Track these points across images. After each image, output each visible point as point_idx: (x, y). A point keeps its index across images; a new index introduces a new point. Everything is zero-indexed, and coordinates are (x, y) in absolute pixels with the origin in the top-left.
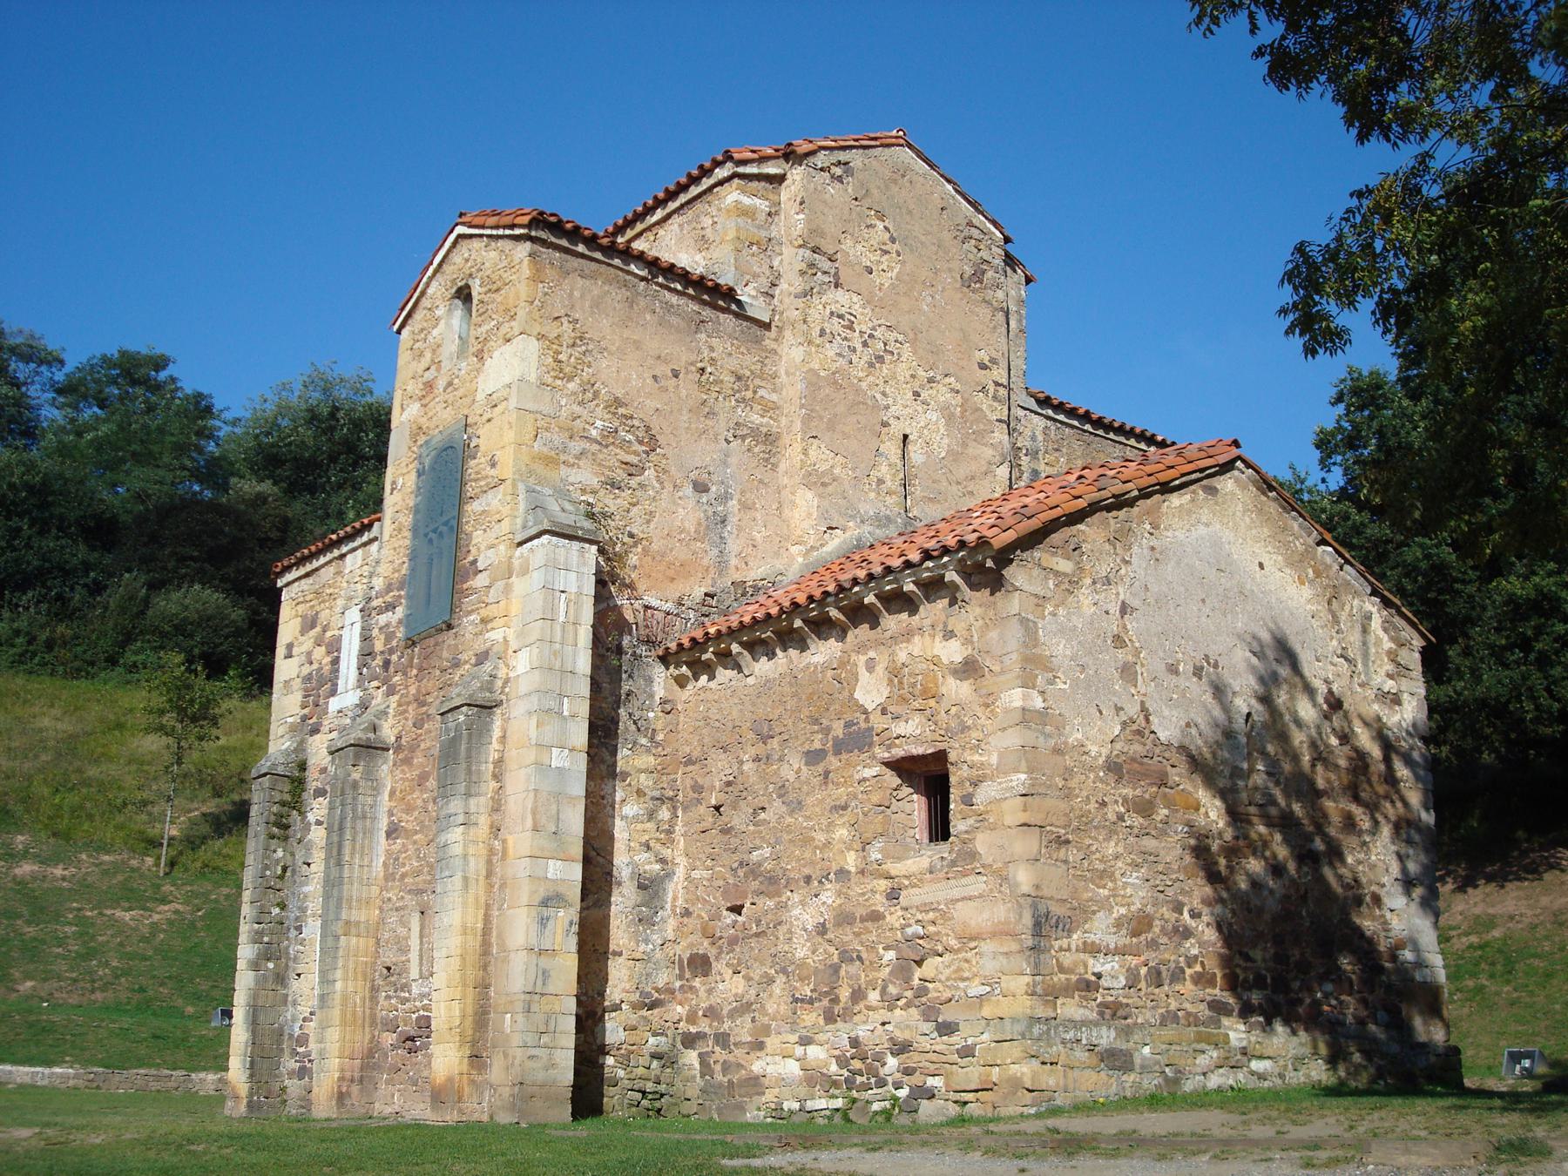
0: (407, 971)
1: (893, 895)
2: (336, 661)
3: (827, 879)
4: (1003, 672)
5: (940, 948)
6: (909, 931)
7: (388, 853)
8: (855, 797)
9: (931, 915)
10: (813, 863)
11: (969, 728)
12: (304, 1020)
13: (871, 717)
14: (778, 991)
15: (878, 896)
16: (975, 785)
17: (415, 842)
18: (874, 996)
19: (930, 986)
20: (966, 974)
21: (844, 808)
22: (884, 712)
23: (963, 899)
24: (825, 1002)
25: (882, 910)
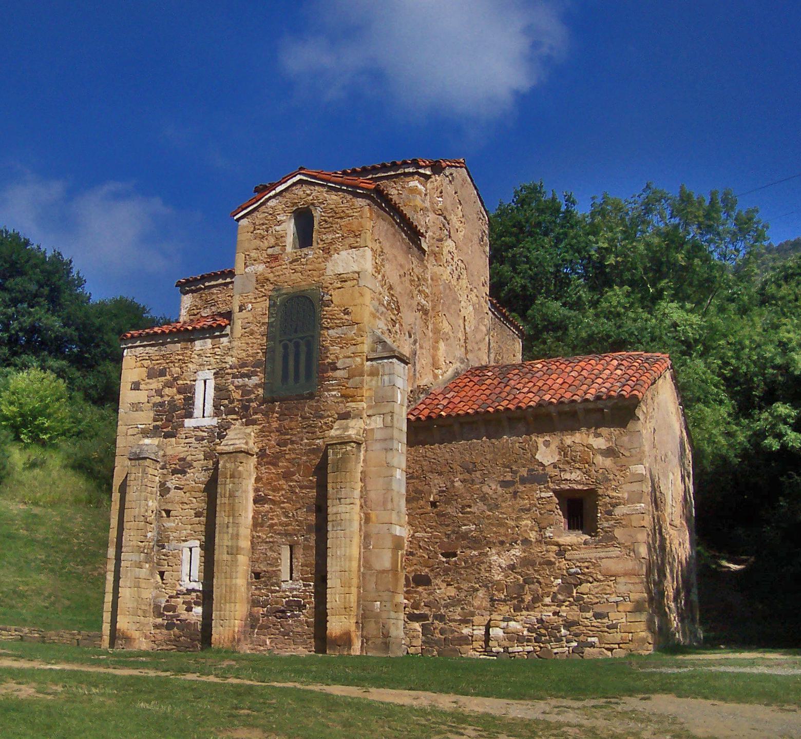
0: (277, 576)
1: (561, 553)
3: (516, 543)
4: (631, 456)
5: (591, 579)
6: (572, 571)
7: (256, 512)
8: (535, 506)
9: (586, 564)
10: (506, 535)
11: (610, 480)
12: (171, 597)
13: (547, 469)
14: (481, 595)
15: (551, 553)
16: (615, 505)
17: (283, 508)
18: (548, 600)
19: (585, 596)
20: (608, 592)
21: (529, 510)
22: (555, 467)
23: (607, 558)
24: (516, 602)
25: (553, 560)
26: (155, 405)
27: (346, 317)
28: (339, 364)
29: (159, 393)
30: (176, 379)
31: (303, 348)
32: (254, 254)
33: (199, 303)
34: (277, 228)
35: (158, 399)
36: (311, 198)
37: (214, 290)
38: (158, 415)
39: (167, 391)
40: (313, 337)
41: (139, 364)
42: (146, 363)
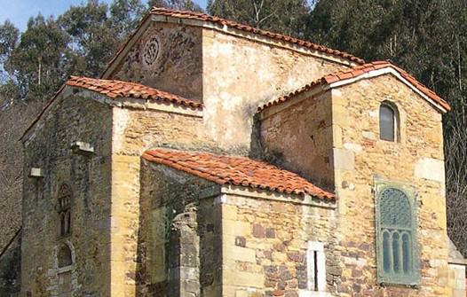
26: (265, 267)
27: (434, 220)
28: (432, 263)
29: (269, 255)
30: (286, 244)
31: (400, 241)
32: (350, 131)
33: (139, 126)
34: (372, 114)
35: (268, 263)
36: (398, 95)
37: (156, 115)
38: (270, 280)
39: (276, 255)
40: (409, 232)
41: (242, 217)
42: (251, 218)
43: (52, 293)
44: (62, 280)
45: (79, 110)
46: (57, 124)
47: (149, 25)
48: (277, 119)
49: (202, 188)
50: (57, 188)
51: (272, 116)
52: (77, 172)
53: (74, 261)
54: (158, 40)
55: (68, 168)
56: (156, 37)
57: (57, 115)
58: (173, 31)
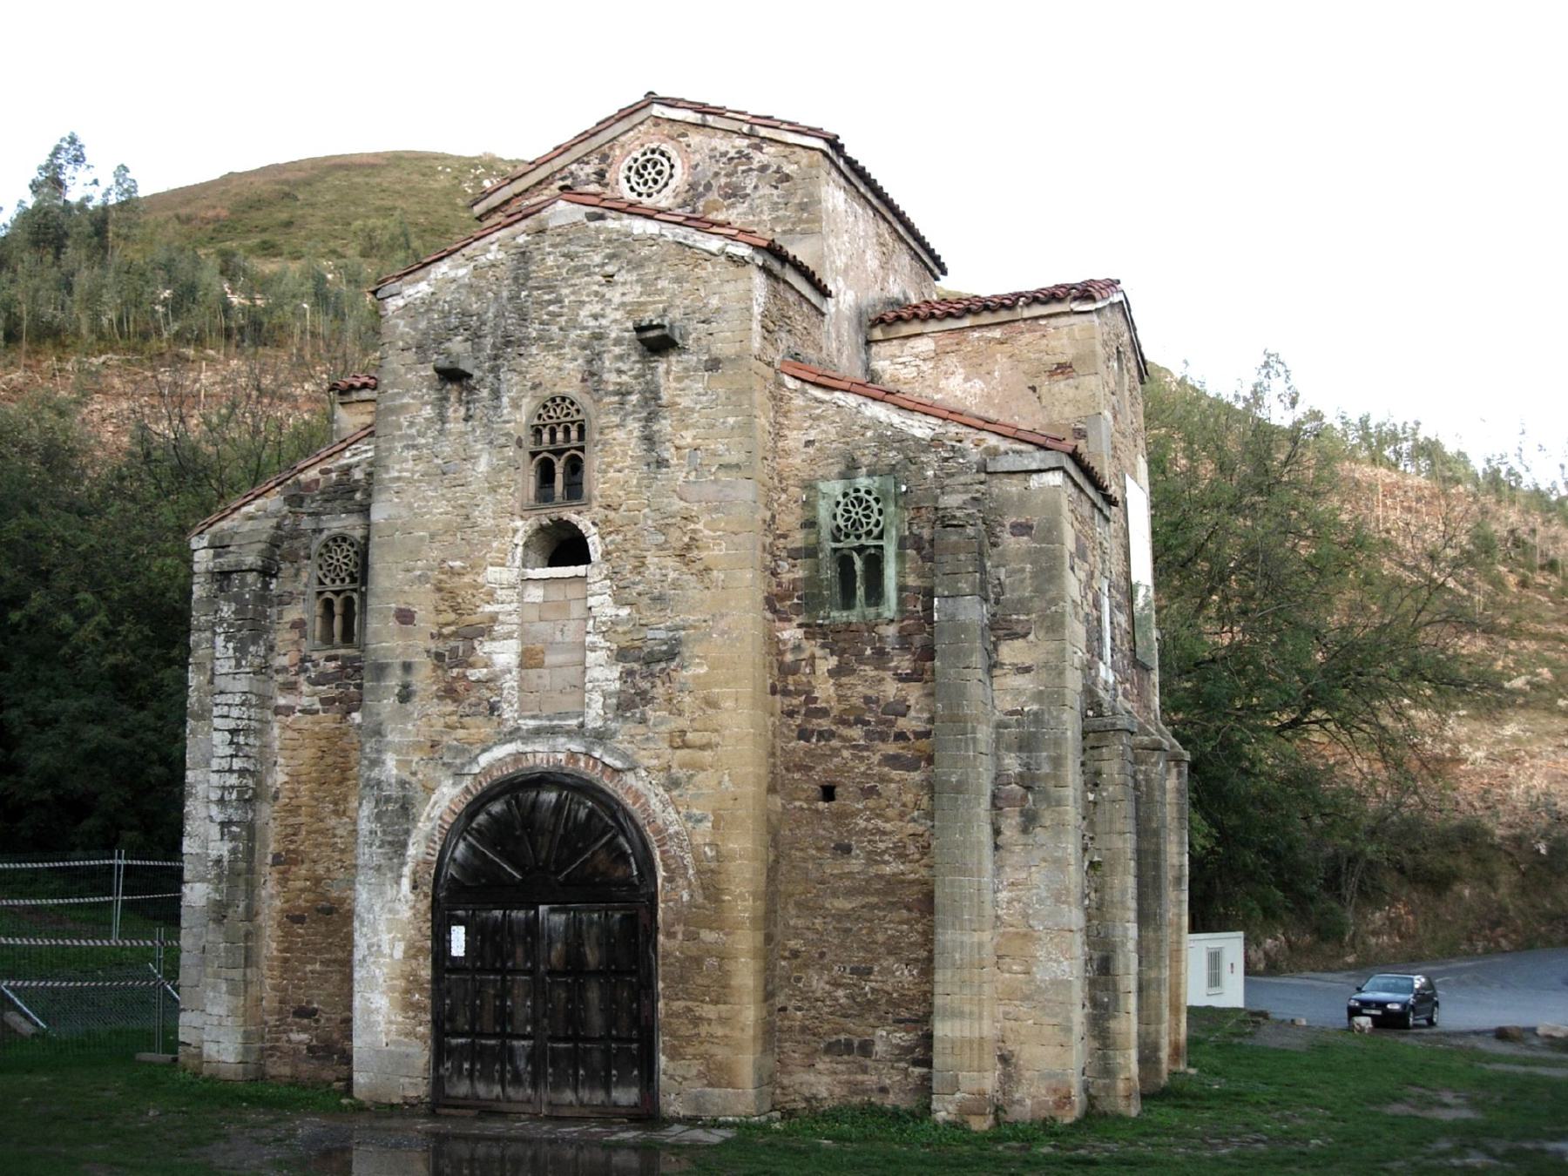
2: (1099, 620)
43: (500, 617)
44: (535, 594)
45: (612, 257)
46: (521, 278)
47: (642, 123)
48: (925, 345)
49: (994, 453)
50: (528, 404)
51: (908, 337)
52: (612, 378)
53: (595, 556)
54: (673, 154)
55: (574, 367)
56: (664, 147)
57: (523, 256)
58: (723, 144)
